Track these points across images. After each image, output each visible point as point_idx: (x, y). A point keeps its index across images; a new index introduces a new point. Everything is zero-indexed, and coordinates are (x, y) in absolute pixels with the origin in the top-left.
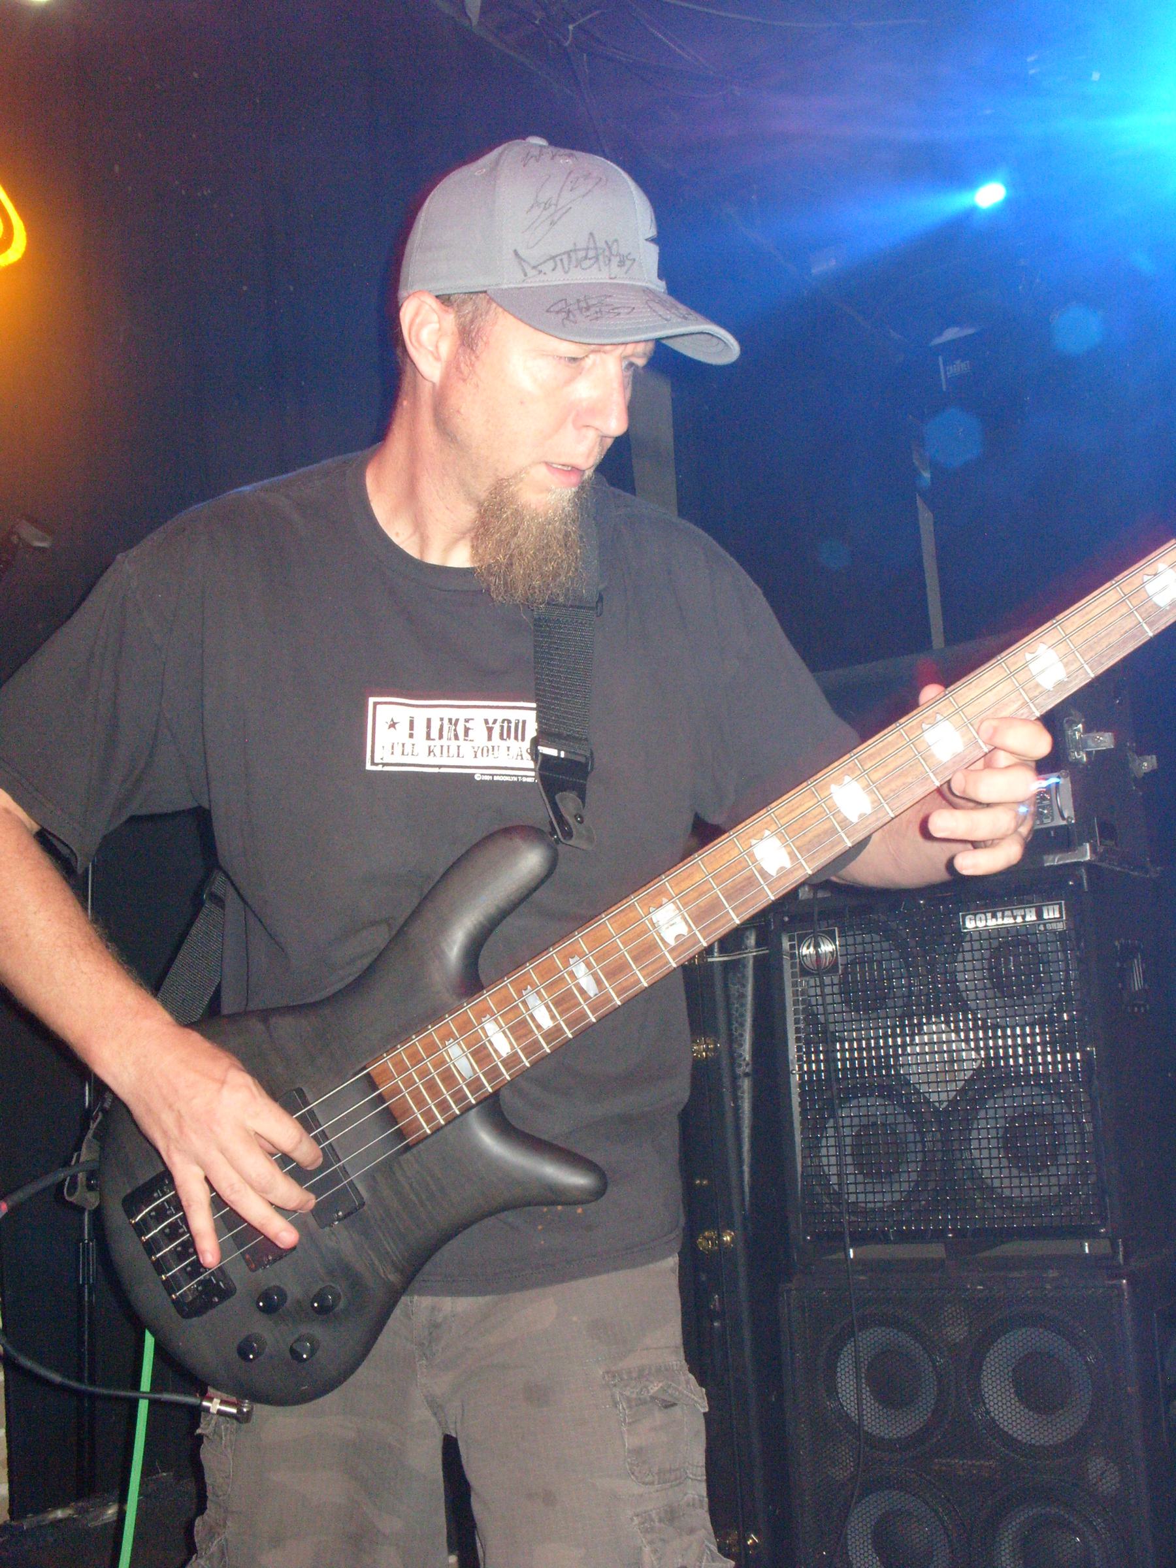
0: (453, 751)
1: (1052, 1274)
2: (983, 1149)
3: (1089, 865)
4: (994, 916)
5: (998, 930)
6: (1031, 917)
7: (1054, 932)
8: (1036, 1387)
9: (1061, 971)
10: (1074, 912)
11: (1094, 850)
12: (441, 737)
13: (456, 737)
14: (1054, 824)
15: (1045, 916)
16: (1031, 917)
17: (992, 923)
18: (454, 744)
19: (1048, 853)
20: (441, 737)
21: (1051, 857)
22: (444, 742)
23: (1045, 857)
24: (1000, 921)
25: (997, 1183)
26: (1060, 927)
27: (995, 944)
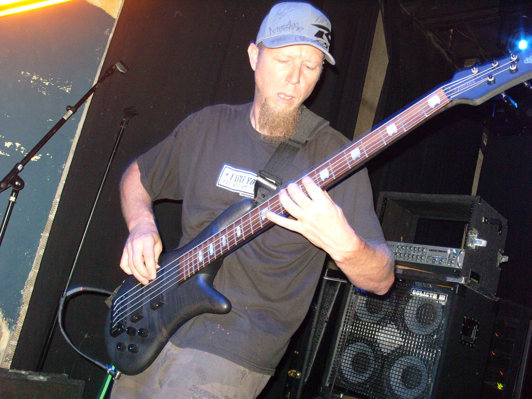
3: (461, 286)
4: (423, 293)
5: (423, 298)
6: (435, 297)
7: (441, 304)
9: (440, 320)
11: (466, 281)
14: (455, 267)
15: (440, 298)
17: (421, 295)
21: (450, 278)
23: (448, 278)
24: (424, 295)
26: (443, 304)
27: (423, 303)
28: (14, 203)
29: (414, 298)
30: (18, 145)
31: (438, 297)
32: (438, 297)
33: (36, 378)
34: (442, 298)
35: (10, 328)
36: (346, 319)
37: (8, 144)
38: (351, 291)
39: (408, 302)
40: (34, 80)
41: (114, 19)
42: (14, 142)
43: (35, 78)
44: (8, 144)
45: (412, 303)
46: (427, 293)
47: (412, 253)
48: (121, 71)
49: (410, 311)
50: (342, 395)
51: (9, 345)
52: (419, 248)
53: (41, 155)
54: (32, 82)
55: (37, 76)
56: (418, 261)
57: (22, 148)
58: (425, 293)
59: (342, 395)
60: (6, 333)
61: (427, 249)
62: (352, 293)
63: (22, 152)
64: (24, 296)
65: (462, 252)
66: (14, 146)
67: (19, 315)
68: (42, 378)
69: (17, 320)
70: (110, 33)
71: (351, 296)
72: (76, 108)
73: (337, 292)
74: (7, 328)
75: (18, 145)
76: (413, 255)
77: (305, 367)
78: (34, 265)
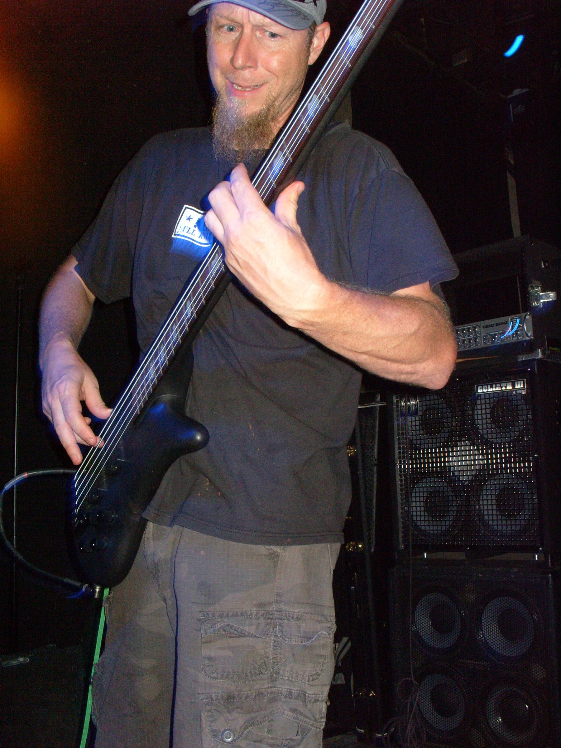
1: (515, 570)
2: (487, 505)
3: (540, 361)
4: (492, 387)
5: (494, 393)
6: (509, 387)
7: (520, 394)
8: (508, 627)
9: (525, 415)
10: (530, 385)
11: (543, 353)
14: (524, 339)
15: (516, 387)
16: (509, 387)
17: (490, 390)
19: (519, 354)
21: (522, 356)
23: (519, 356)
24: (494, 389)
25: (491, 523)
26: (523, 392)
27: (496, 399)
29: (483, 397)
31: (513, 386)
32: (513, 386)
33: (14, 663)
34: (519, 386)
36: (400, 453)
38: (395, 414)
39: (476, 404)
45: (481, 404)
46: (498, 385)
47: (461, 338)
49: (482, 416)
50: (425, 554)
52: (469, 329)
56: (473, 347)
58: (494, 386)
59: (425, 554)
61: (479, 327)
62: (398, 416)
65: (527, 317)
68: (21, 659)
71: (398, 420)
73: (377, 422)
76: (464, 341)
77: (366, 534)
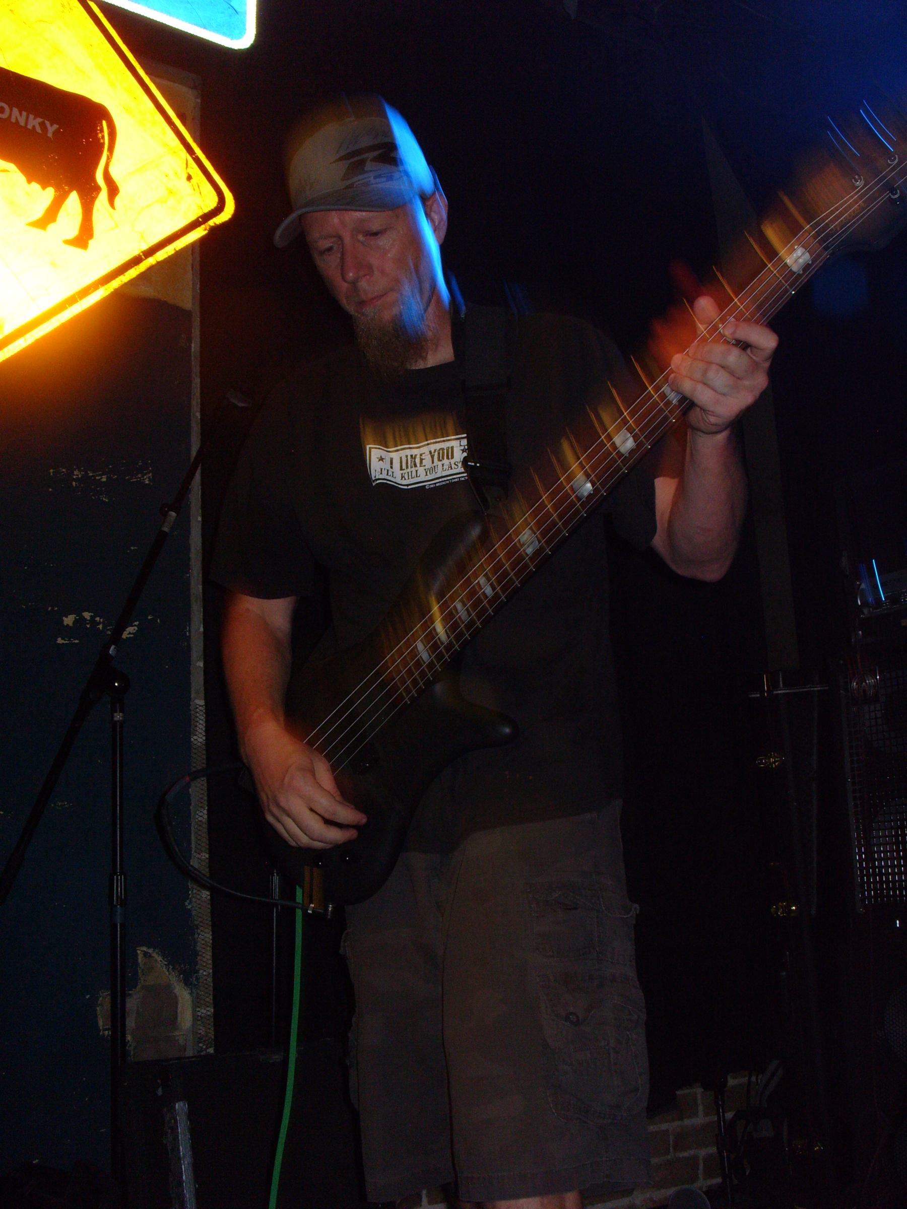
0: (414, 474)
12: (407, 467)
13: (415, 466)
18: (414, 469)
20: (407, 467)
22: (409, 470)
28: (121, 723)
30: (87, 615)
35: (187, 983)
37: (69, 620)
40: (76, 480)
41: (188, 314)
42: (79, 614)
43: (77, 474)
44: (69, 620)
48: (241, 405)
51: (195, 1018)
53: (137, 623)
54: (74, 483)
55: (80, 471)
57: (98, 619)
60: (184, 996)
63: (101, 626)
64: (194, 913)
66: (80, 621)
67: (196, 953)
69: (196, 964)
70: (189, 340)
72: (180, 503)
74: (182, 984)
75: (87, 615)
78: (193, 846)
